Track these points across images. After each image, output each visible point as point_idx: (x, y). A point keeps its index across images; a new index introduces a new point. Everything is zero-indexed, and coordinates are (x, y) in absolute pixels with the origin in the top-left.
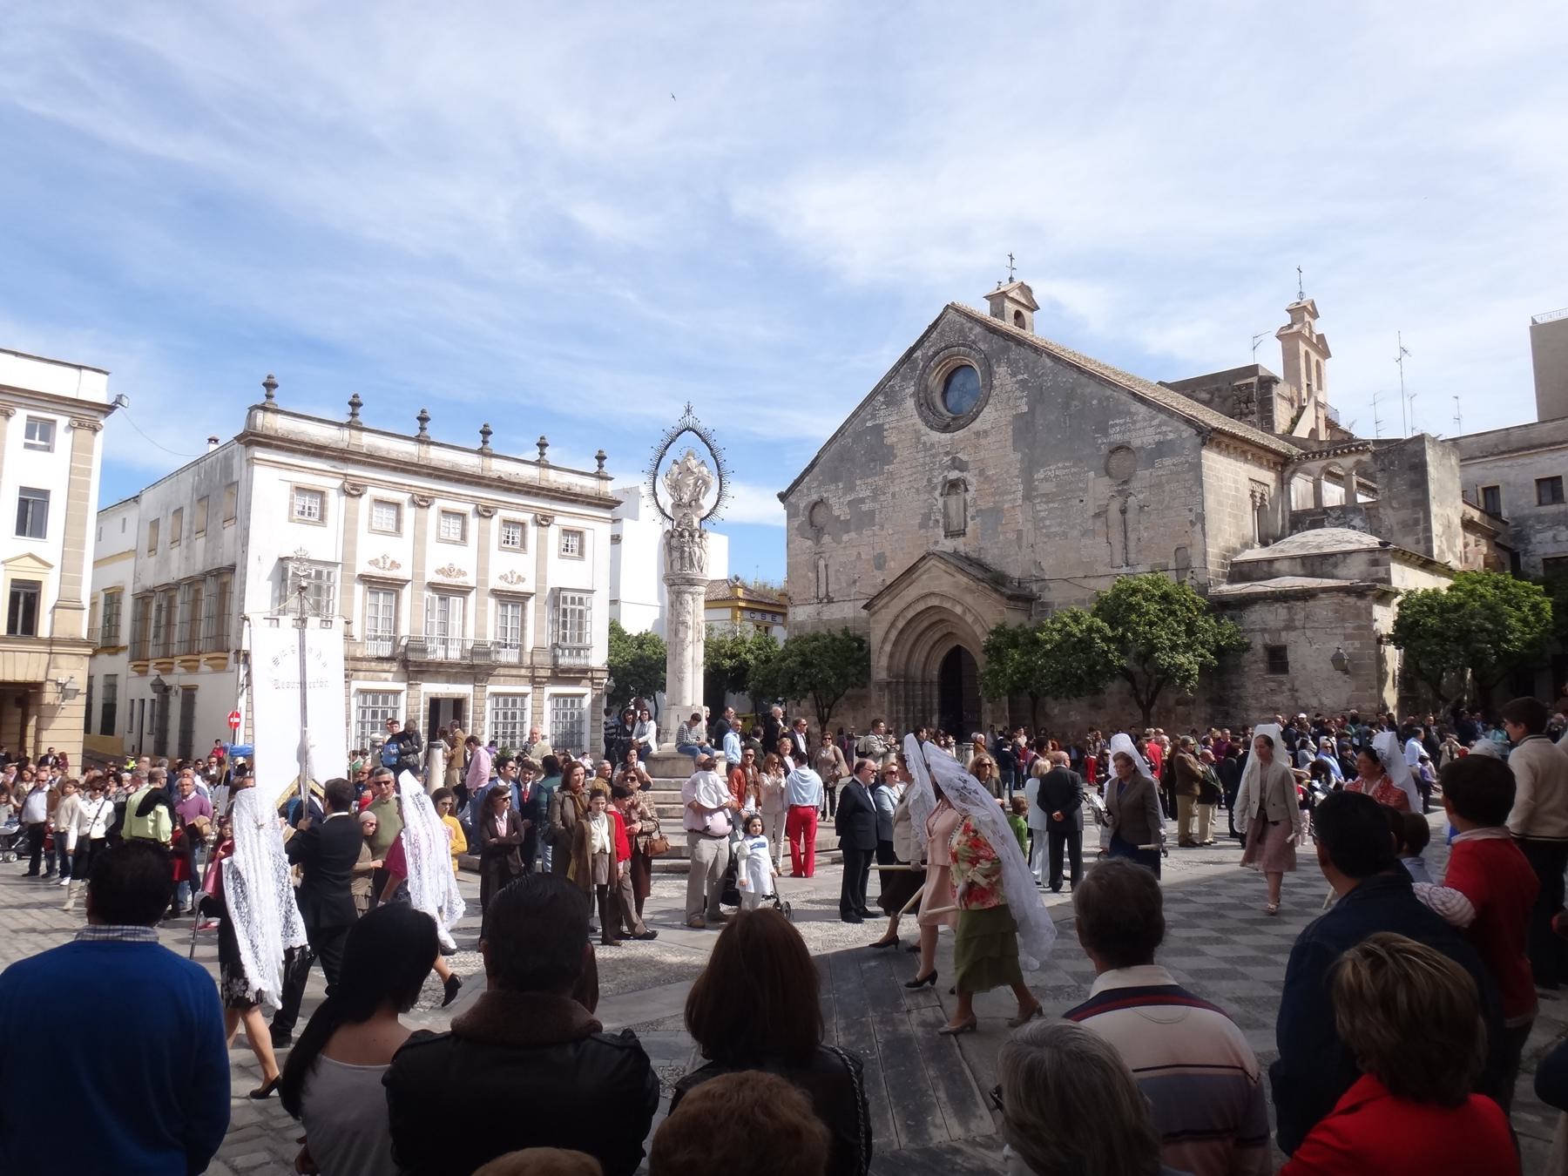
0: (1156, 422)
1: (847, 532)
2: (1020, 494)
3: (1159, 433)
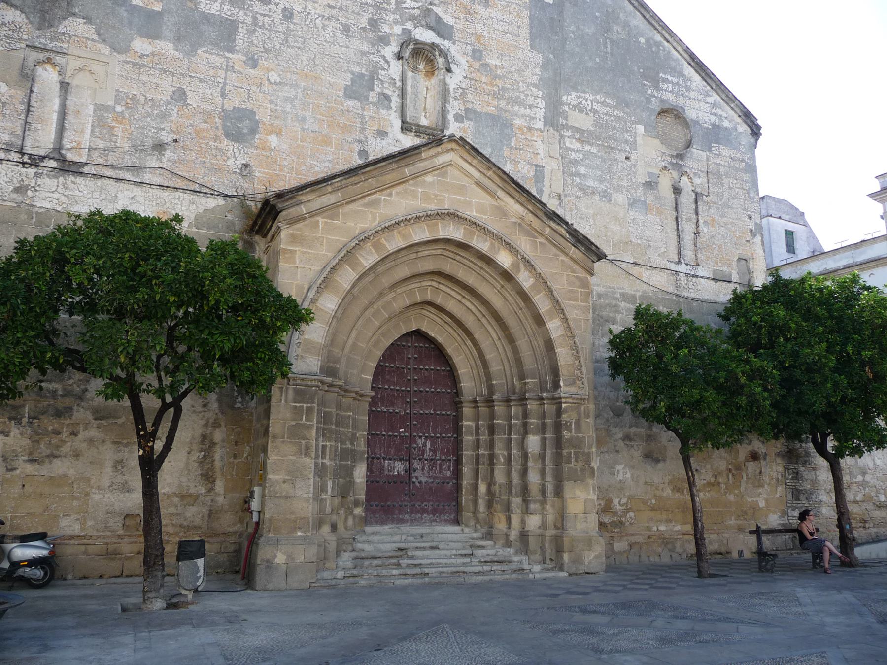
0: (710, 100)
1: (153, 35)
2: (540, 114)
3: (715, 115)
